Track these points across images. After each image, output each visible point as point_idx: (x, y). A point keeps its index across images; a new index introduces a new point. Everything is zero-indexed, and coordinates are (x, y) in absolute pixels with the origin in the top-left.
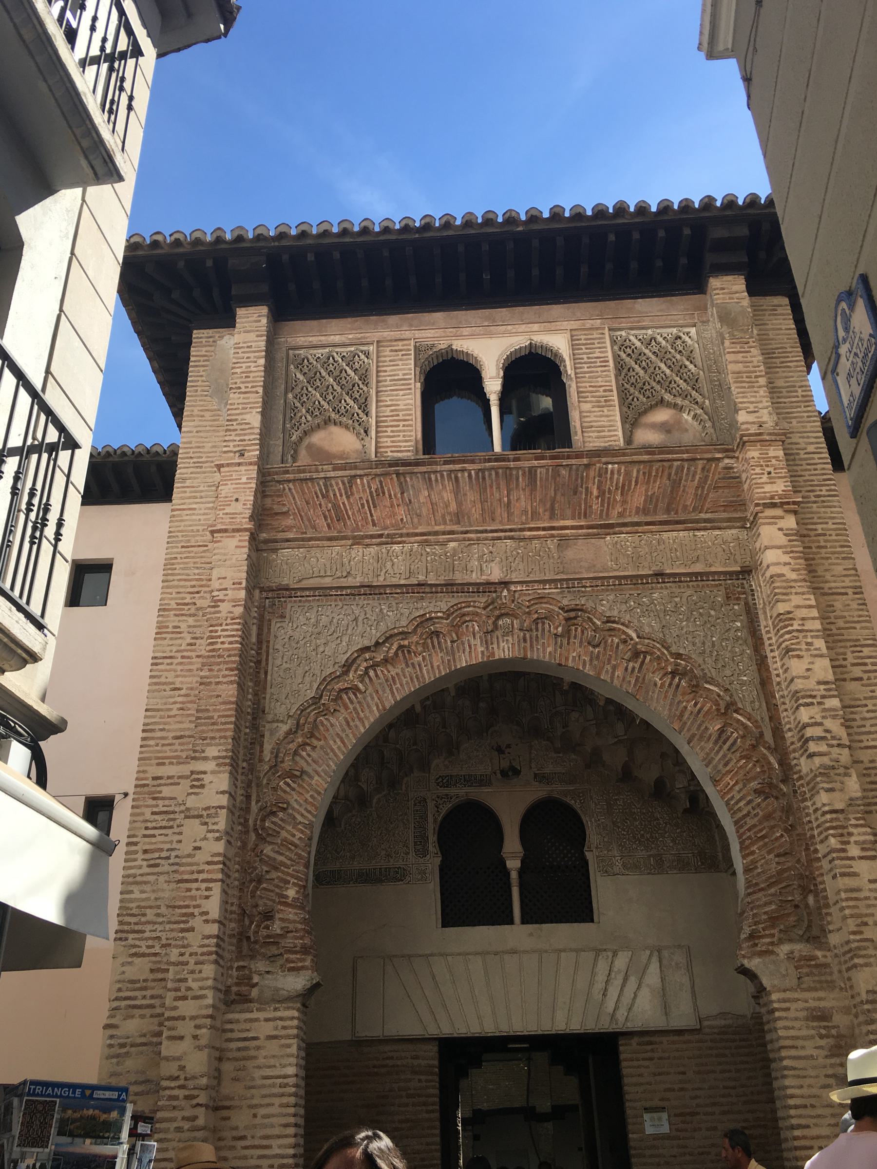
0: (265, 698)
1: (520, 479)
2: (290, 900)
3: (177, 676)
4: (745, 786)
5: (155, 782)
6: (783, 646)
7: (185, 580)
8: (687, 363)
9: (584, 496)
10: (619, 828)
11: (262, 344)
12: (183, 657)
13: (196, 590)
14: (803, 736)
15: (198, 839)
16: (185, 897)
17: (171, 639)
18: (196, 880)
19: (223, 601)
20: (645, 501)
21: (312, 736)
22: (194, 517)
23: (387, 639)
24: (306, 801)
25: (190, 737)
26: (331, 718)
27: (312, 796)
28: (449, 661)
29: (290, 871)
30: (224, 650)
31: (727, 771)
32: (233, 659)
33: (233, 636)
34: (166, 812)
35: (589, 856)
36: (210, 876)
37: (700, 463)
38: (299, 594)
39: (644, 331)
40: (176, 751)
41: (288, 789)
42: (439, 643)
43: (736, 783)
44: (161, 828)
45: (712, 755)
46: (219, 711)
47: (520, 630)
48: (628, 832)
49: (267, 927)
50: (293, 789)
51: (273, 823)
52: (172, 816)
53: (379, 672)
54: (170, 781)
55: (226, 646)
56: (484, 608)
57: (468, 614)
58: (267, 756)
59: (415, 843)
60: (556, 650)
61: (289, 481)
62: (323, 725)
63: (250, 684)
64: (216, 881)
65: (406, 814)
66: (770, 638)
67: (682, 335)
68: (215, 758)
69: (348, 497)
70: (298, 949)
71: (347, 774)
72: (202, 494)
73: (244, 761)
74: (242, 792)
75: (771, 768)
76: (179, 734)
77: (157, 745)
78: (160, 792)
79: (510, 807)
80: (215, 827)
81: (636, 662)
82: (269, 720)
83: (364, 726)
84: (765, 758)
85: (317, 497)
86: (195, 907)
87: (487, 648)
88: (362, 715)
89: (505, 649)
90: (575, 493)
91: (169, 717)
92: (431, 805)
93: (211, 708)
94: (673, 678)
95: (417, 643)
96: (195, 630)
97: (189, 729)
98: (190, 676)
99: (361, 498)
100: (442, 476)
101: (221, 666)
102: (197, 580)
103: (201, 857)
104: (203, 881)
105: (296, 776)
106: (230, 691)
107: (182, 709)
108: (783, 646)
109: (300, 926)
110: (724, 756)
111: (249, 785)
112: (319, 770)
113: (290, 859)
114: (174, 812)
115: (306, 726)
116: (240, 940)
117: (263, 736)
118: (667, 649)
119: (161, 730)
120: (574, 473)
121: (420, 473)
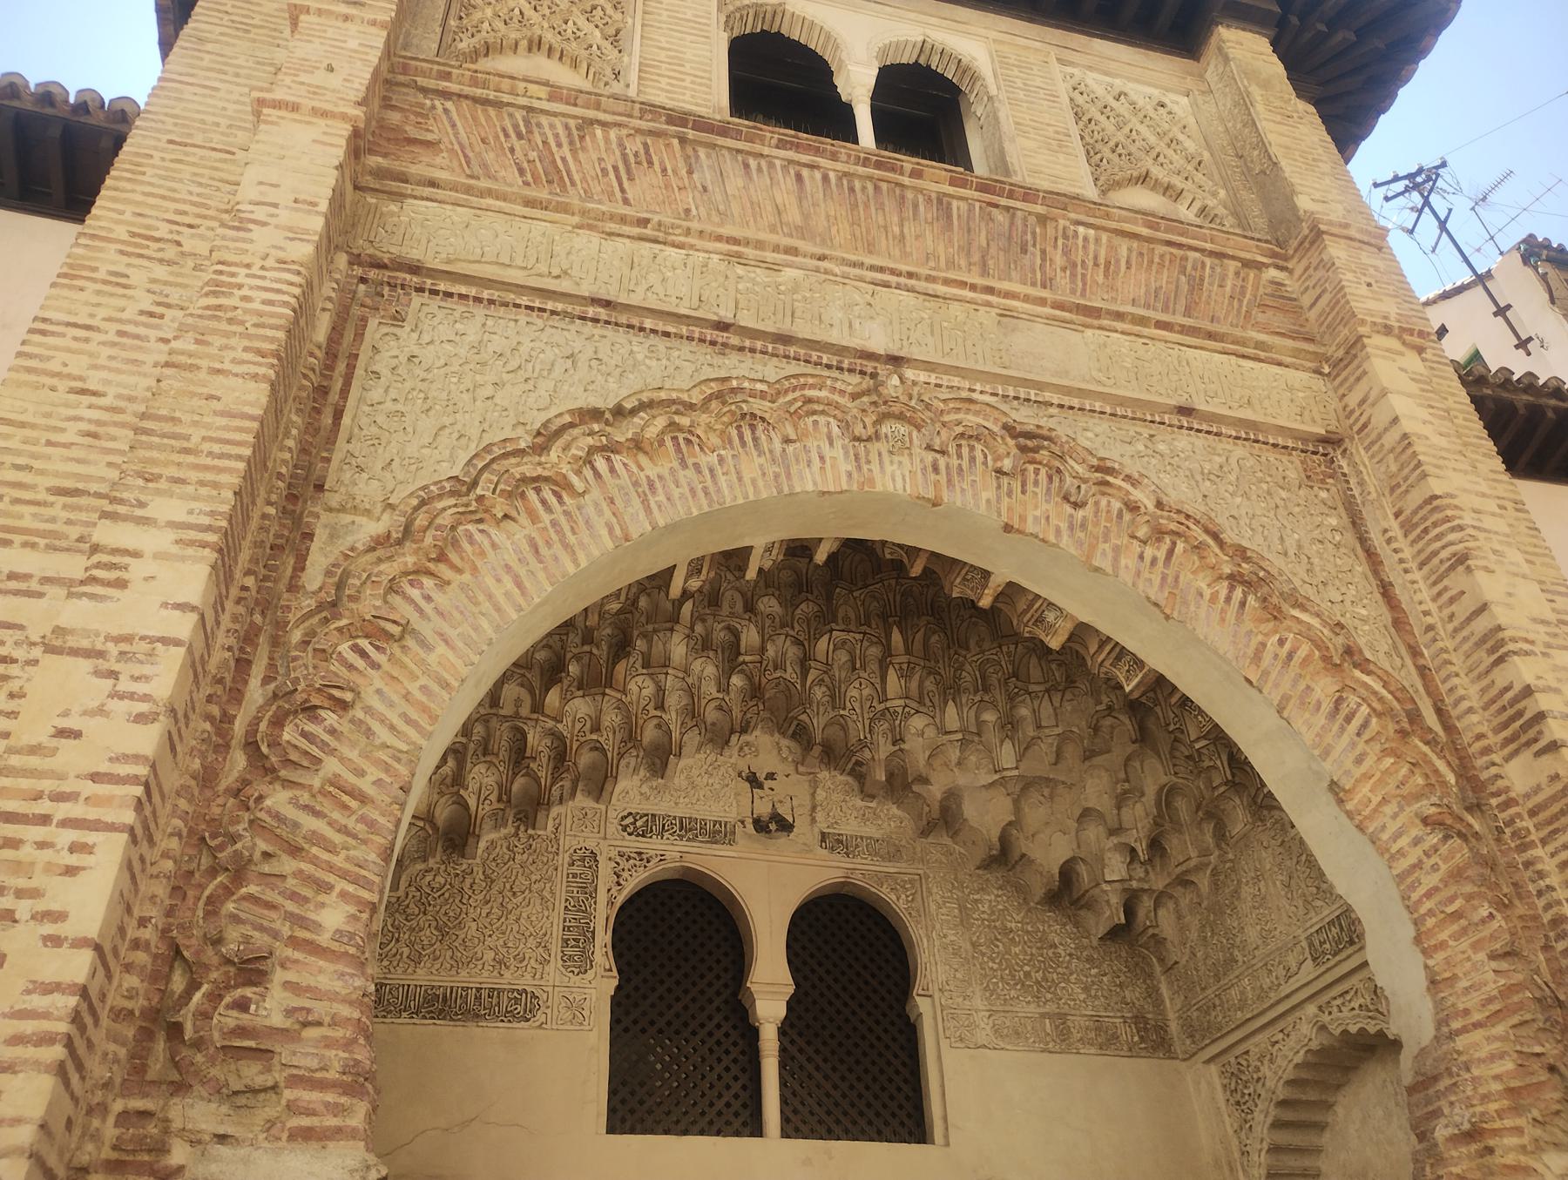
0: (328, 460)
1: (922, 208)
2: (324, 939)
3: (95, 367)
4: (1402, 809)
6: (1444, 554)
7: (163, 197)
8: (1181, 137)
9: (1039, 262)
10: (984, 955)
12: (121, 333)
13: (187, 220)
14: (1520, 714)
15: (76, 709)
18: (45, 820)
19: (264, 224)
20: (1147, 293)
21: (441, 558)
22: (210, 101)
23: (642, 406)
24: (407, 697)
25: (98, 495)
26: (493, 531)
27: (424, 688)
28: (777, 476)
29: (338, 861)
30: (246, 311)
31: (1364, 775)
32: (270, 333)
33: (278, 291)
35: (923, 1005)
37: (1233, 266)
38: (442, 287)
40: (53, 520)
41: (360, 663)
42: (755, 439)
43: (1384, 801)
45: (1329, 739)
46: (208, 426)
47: (929, 448)
48: (1000, 963)
49: (242, 1005)
50: (375, 666)
51: (304, 734)
53: (618, 466)
54: (13, 585)
55: (256, 305)
56: (854, 397)
57: (818, 401)
58: (313, 577)
59: (566, 941)
60: (999, 499)
61: (446, 95)
62: (471, 541)
63: (294, 418)
64: (111, 827)
65: (549, 880)
66: (1399, 553)
67: (1167, 101)
69: (574, 151)
70: (332, 1075)
71: (493, 697)
73: (248, 573)
74: (232, 641)
75: (1444, 784)
76: (69, 484)
79: (769, 893)
80: (141, 688)
82: (334, 504)
83: (575, 562)
84: (1430, 763)
85: (507, 135)
86: (20, 894)
87: (859, 468)
88: (572, 539)
89: (898, 474)
90: (1024, 251)
91: (49, 443)
92: (605, 870)
94: (1232, 589)
96: (167, 290)
97: (102, 479)
99: (600, 160)
100: (771, 166)
101: (233, 341)
103: (71, 757)
104: (66, 823)
105: (389, 636)
107: (95, 436)
108: (1444, 554)
109: (346, 1011)
110: (1353, 745)
111: (249, 637)
112: (452, 633)
116: (146, 1035)
117: (309, 536)
118: (1215, 536)
120: (1019, 222)
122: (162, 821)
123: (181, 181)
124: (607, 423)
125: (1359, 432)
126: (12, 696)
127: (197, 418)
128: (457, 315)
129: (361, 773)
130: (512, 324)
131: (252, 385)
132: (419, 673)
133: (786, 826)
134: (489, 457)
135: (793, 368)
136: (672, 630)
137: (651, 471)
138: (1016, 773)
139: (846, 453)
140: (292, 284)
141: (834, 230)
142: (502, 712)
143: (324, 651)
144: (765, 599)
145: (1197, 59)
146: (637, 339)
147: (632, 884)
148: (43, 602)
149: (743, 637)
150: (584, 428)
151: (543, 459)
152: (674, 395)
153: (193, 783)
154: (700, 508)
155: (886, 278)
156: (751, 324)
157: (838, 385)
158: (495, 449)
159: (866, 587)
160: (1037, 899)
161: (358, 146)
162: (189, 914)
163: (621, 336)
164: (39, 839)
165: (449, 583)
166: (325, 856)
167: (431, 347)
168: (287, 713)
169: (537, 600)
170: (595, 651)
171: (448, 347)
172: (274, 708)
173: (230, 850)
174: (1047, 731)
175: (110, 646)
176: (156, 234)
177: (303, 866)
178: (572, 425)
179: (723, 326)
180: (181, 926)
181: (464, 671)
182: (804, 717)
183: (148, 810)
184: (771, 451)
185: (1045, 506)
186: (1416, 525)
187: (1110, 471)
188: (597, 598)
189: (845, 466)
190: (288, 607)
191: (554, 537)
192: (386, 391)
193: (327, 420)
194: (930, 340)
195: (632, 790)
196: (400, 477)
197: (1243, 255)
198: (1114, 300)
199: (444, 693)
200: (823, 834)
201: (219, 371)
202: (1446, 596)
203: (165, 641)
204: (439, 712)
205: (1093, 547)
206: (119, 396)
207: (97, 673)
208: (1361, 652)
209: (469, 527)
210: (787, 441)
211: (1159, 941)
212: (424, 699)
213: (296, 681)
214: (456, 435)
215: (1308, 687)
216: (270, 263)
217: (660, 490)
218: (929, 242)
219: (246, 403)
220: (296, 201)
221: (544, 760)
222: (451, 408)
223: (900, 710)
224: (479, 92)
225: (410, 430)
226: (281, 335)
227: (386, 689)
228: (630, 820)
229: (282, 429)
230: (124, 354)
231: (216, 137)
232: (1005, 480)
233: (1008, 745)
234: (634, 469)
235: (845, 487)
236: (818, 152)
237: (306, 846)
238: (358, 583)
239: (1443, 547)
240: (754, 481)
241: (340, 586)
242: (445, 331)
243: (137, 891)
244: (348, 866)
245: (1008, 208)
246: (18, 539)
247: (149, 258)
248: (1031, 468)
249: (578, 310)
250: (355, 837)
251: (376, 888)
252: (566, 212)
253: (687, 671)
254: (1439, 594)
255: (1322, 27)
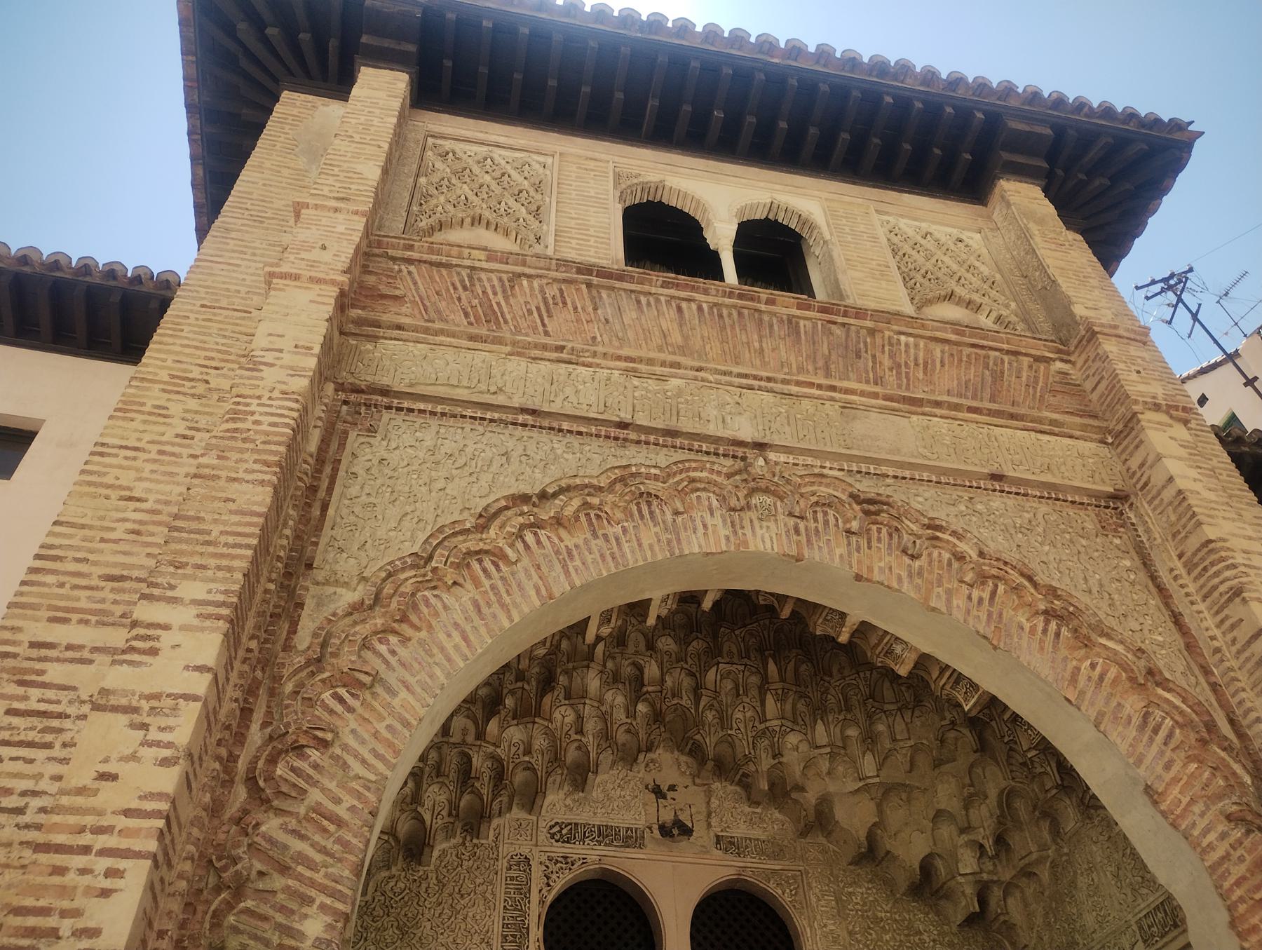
0: (316, 544)
1: (776, 327)
3: (140, 479)
5: (35, 653)
6: (1222, 588)
7: (197, 348)
8: (977, 264)
9: (870, 364)
10: (859, 942)
11: (396, 104)
12: (160, 452)
13: (214, 364)
15: (114, 756)
16: (45, 888)
17: (145, 422)
18: (86, 850)
19: (272, 365)
20: (959, 384)
21: (404, 619)
22: (234, 275)
23: (562, 490)
24: (376, 735)
25: (139, 580)
26: (444, 596)
27: (389, 727)
28: (669, 541)
29: (319, 877)
30: (256, 432)
32: (273, 448)
33: (282, 416)
34: (44, 714)
36: (124, 844)
37: (1026, 361)
38: (405, 405)
39: (917, 223)
40: (103, 601)
41: (339, 708)
42: (651, 513)
44: (21, 744)
46: (225, 523)
47: (791, 514)
50: (351, 710)
51: (293, 769)
52: (55, 723)
54: (70, 654)
55: (264, 427)
56: (729, 476)
58: (303, 639)
61: (410, 261)
63: (291, 512)
64: (138, 855)
65: (491, 883)
66: (1185, 588)
67: (964, 237)
68: (195, 602)
69: (506, 298)
71: (445, 729)
72: (257, 252)
73: (252, 637)
74: (238, 694)
77: (62, 585)
78: (41, 672)
79: (674, 889)
80: (166, 737)
81: (983, 590)
82: (320, 579)
85: (455, 288)
87: (735, 533)
88: (507, 599)
91: (102, 540)
92: (537, 872)
93: (208, 517)
94: (1047, 622)
95: (615, 505)
96: (197, 417)
98: (168, 483)
100: (657, 301)
101: (246, 456)
102: (219, 351)
103: (110, 796)
104: (104, 852)
105: (362, 685)
106: (259, 498)
108: (1222, 588)
111: (251, 690)
112: (412, 680)
113: (323, 851)
114: (61, 716)
115: (395, 600)
117: (301, 606)
118: (1030, 579)
119: (77, 560)
120: (853, 335)
121: (625, 290)
122: (178, 847)
123: (210, 335)
124: (534, 505)
125: (1142, 488)
126: (64, 745)
127: (217, 516)
128: (417, 425)
129: (338, 801)
130: (459, 431)
131: (260, 489)
132: (386, 714)
133: (686, 831)
134: (442, 537)
135: (680, 455)
136: (588, 667)
137: (569, 541)
138: (877, 780)
139: (724, 521)
140: (292, 409)
141: (708, 347)
142: (452, 740)
143: (310, 699)
144: (663, 639)
145: (985, 205)
146: (556, 438)
147: (561, 882)
148: (92, 668)
149: (646, 671)
150: (516, 510)
151: (484, 536)
152: (587, 481)
153: (204, 814)
154: (608, 570)
155: (750, 383)
156: (645, 423)
157: (716, 467)
158: (447, 529)
159: (745, 626)
160: (902, 890)
161: (343, 303)
162: (198, 926)
163: (544, 437)
164: (81, 866)
165: (410, 639)
166: (308, 873)
167: (397, 452)
168: (280, 753)
169: (480, 651)
170: (526, 687)
171: (410, 450)
172: (270, 748)
173: (232, 870)
174: (901, 744)
175: (143, 702)
176: (190, 376)
177: (290, 882)
178: (507, 508)
179: (623, 425)
180: (191, 937)
181: (422, 712)
182: (698, 737)
183: (167, 841)
184: (664, 522)
185: (888, 559)
186: (1196, 565)
187: (939, 528)
188: (528, 646)
189: (724, 532)
190: (283, 664)
191: (493, 598)
192: (362, 488)
193: (316, 512)
194: (787, 429)
195: (558, 803)
196: (372, 555)
197: (1033, 352)
198: (933, 391)
199: (405, 730)
200: (718, 837)
201: (235, 479)
202: (1228, 623)
203: (187, 697)
204: (402, 747)
205: (929, 591)
206: (158, 501)
207: (133, 726)
208: (1161, 673)
209: (426, 593)
210: (677, 513)
211: (1010, 927)
212: (389, 736)
213: (288, 725)
214: (416, 520)
215: (1119, 704)
216: (276, 394)
217: (577, 557)
218: (783, 353)
219: (255, 503)
220: (296, 347)
221: (486, 779)
222: (412, 499)
223: (777, 729)
224: (434, 258)
225: (380, 517)
226: (283, 449)
227: (359, 729)
228: (557, 829)
229: (281, 521)
230: (163, 468)
231: (237, 301)
232: (854, 539)
233: (869, 756)
234: (556, 540)
235: (724, 548)
236: (693, 289)
237: (293, 865)
238: (338, 642)
239: (1222, 583)
240: (651, 546)
241: (324, 645)
242: (408, 439)
243: (157, 908)
244: (326, 882)
245: (844, 325)
246: (75, 617)
247: (184, 394)
248: (874, 527)
249: (510, 417)
250: (332, 856)
251: (349, 901)
252: (501, 343)
253: (601, 701)
254: (1222, 622)
255: (1082, 176)
